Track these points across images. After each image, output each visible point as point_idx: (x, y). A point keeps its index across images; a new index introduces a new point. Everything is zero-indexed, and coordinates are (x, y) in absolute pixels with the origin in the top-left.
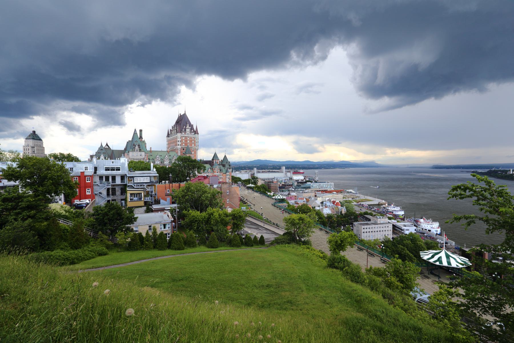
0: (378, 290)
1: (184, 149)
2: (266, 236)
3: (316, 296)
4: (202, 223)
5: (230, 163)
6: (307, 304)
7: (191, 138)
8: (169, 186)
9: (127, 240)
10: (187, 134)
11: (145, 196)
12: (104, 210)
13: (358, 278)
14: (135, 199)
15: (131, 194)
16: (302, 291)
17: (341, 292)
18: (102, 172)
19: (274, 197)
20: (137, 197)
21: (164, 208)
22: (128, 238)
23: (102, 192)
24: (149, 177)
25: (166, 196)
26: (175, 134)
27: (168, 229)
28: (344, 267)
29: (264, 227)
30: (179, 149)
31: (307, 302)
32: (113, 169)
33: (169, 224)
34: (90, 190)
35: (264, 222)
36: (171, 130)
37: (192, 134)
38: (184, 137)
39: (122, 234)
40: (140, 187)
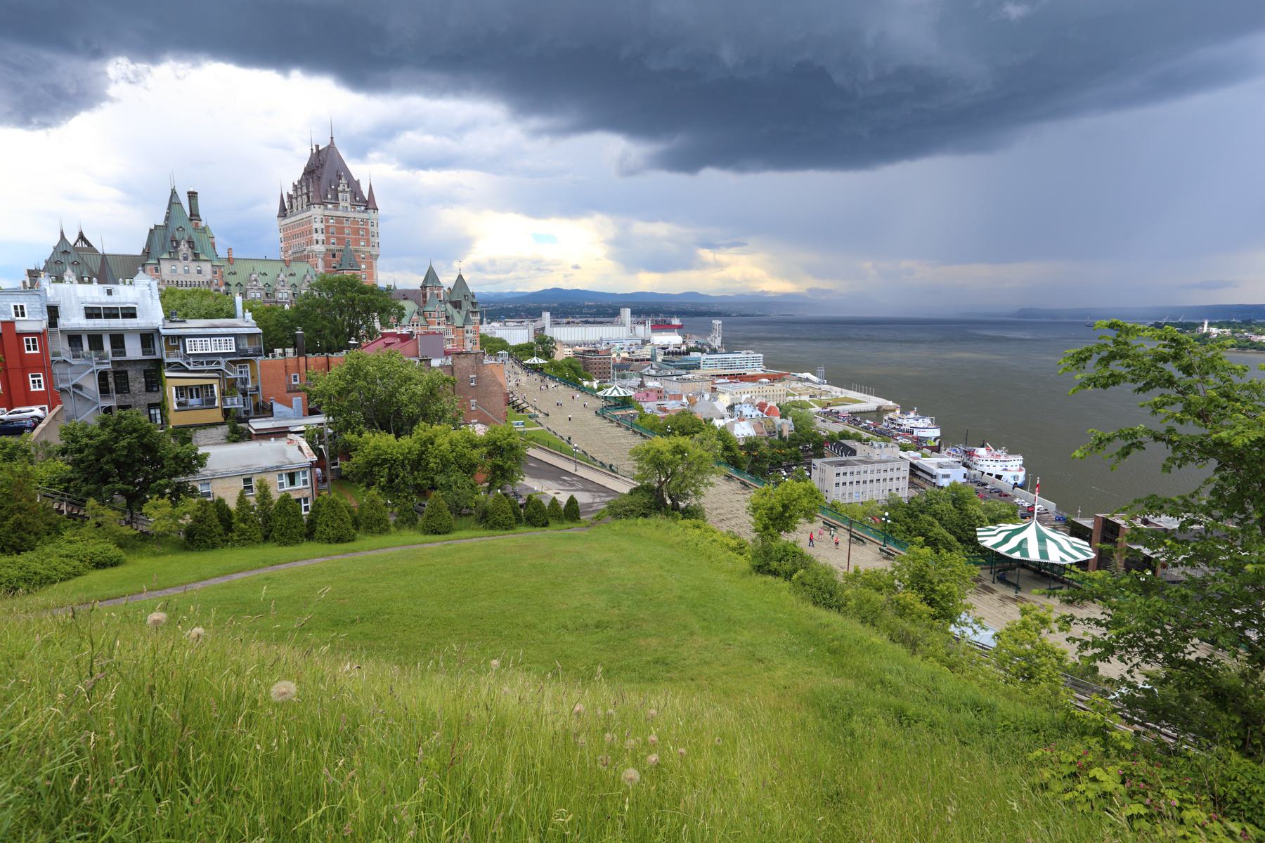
0: (877, 623)
1: (334, 256)
2: (583, 498)
3: (729, 645)
4: (403, 466)
5: (473, 296)
6: (708, 663)
7: (355, 221)
8: (296, 363)
9: (180, 521)
10: (341, 208)
11: (223, 394)
12: (99, 435)
13: (831, 595)
14: (194, 402)
15: (181, 390)
16: (692, 634)
17: (790, 631)
18: (74, 320)
19: (600, 394)
20: (198, 397)
21: (287, 427)
22: (185, 514)
23: (81, 383)
24: (233, 339)
25: (289, 392)
26: (305, 207)
27: (301, 486)
28: (795, 571)
29: (576, 473)
30: (322, 256)
31: (707, 660)
32: (111, 313)
33: (304, 473)
34: (41, 379)
35: (575, 462)
36: (290, 196)
37: (358, 209)
38: (332, 217)
39: (163, 505)
40: (205, 367)
